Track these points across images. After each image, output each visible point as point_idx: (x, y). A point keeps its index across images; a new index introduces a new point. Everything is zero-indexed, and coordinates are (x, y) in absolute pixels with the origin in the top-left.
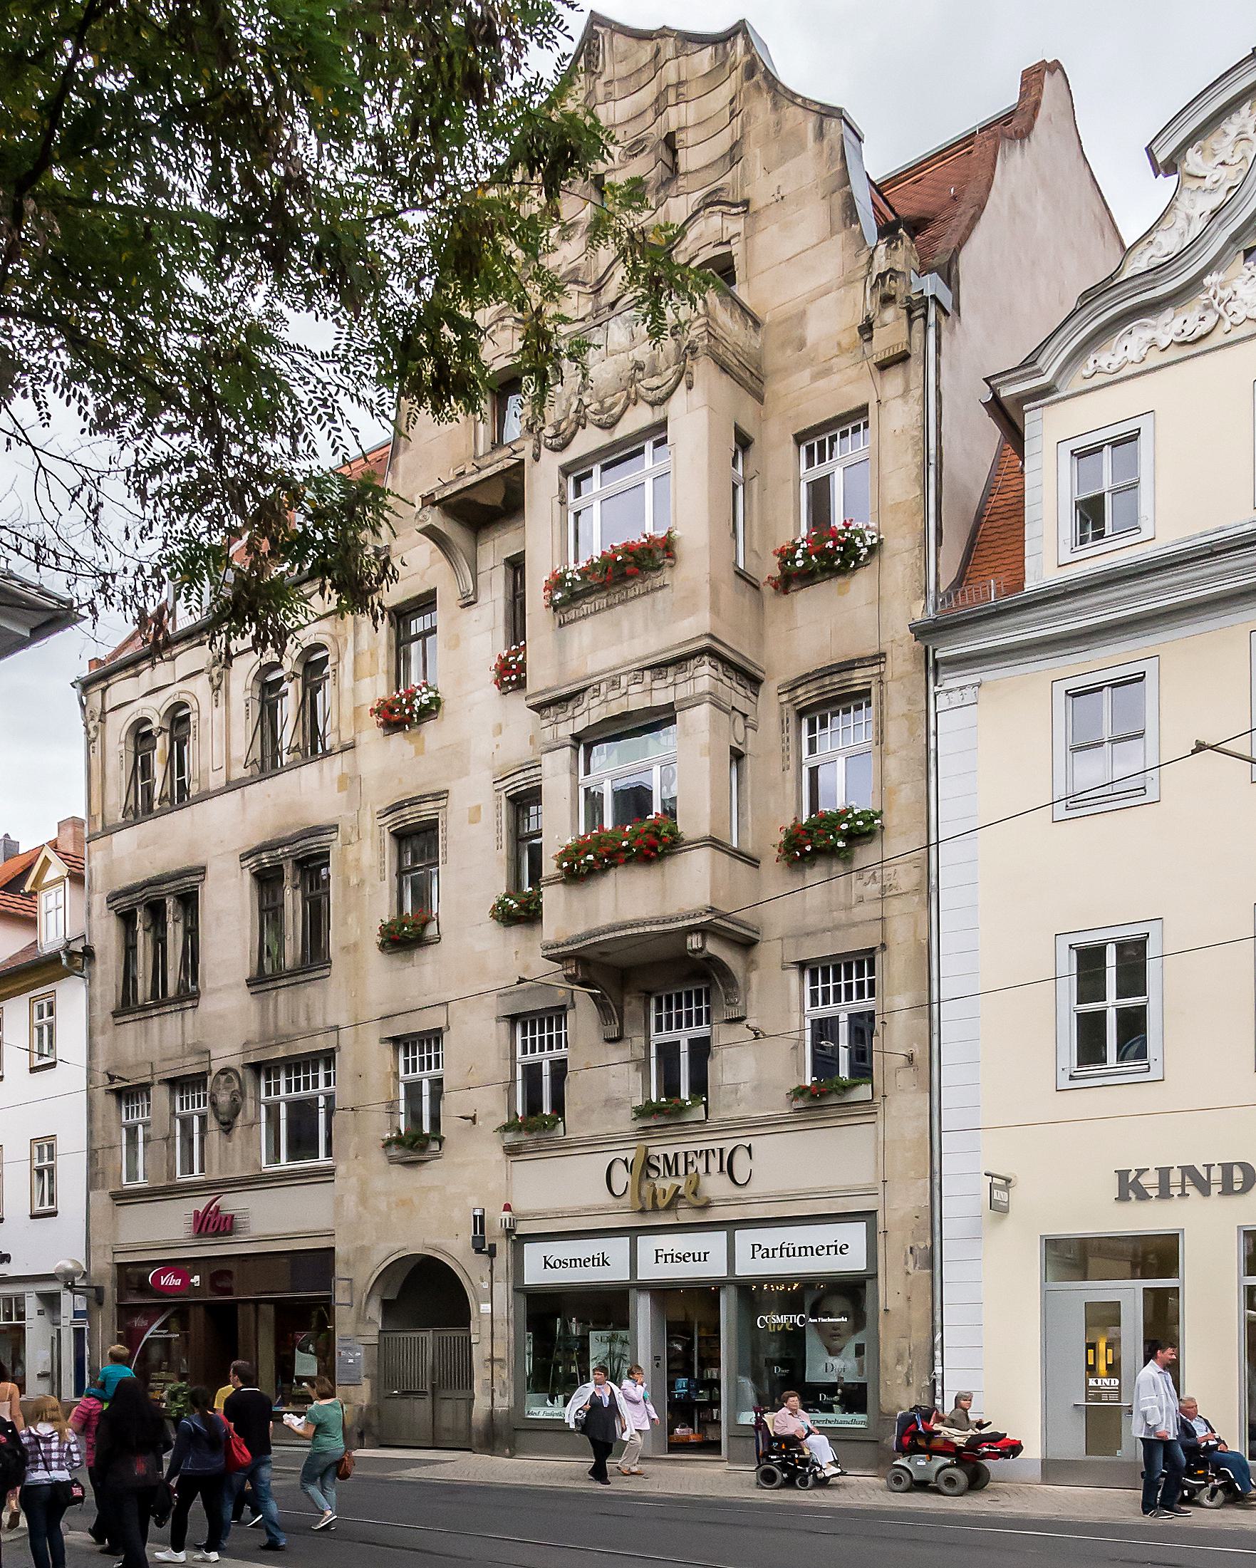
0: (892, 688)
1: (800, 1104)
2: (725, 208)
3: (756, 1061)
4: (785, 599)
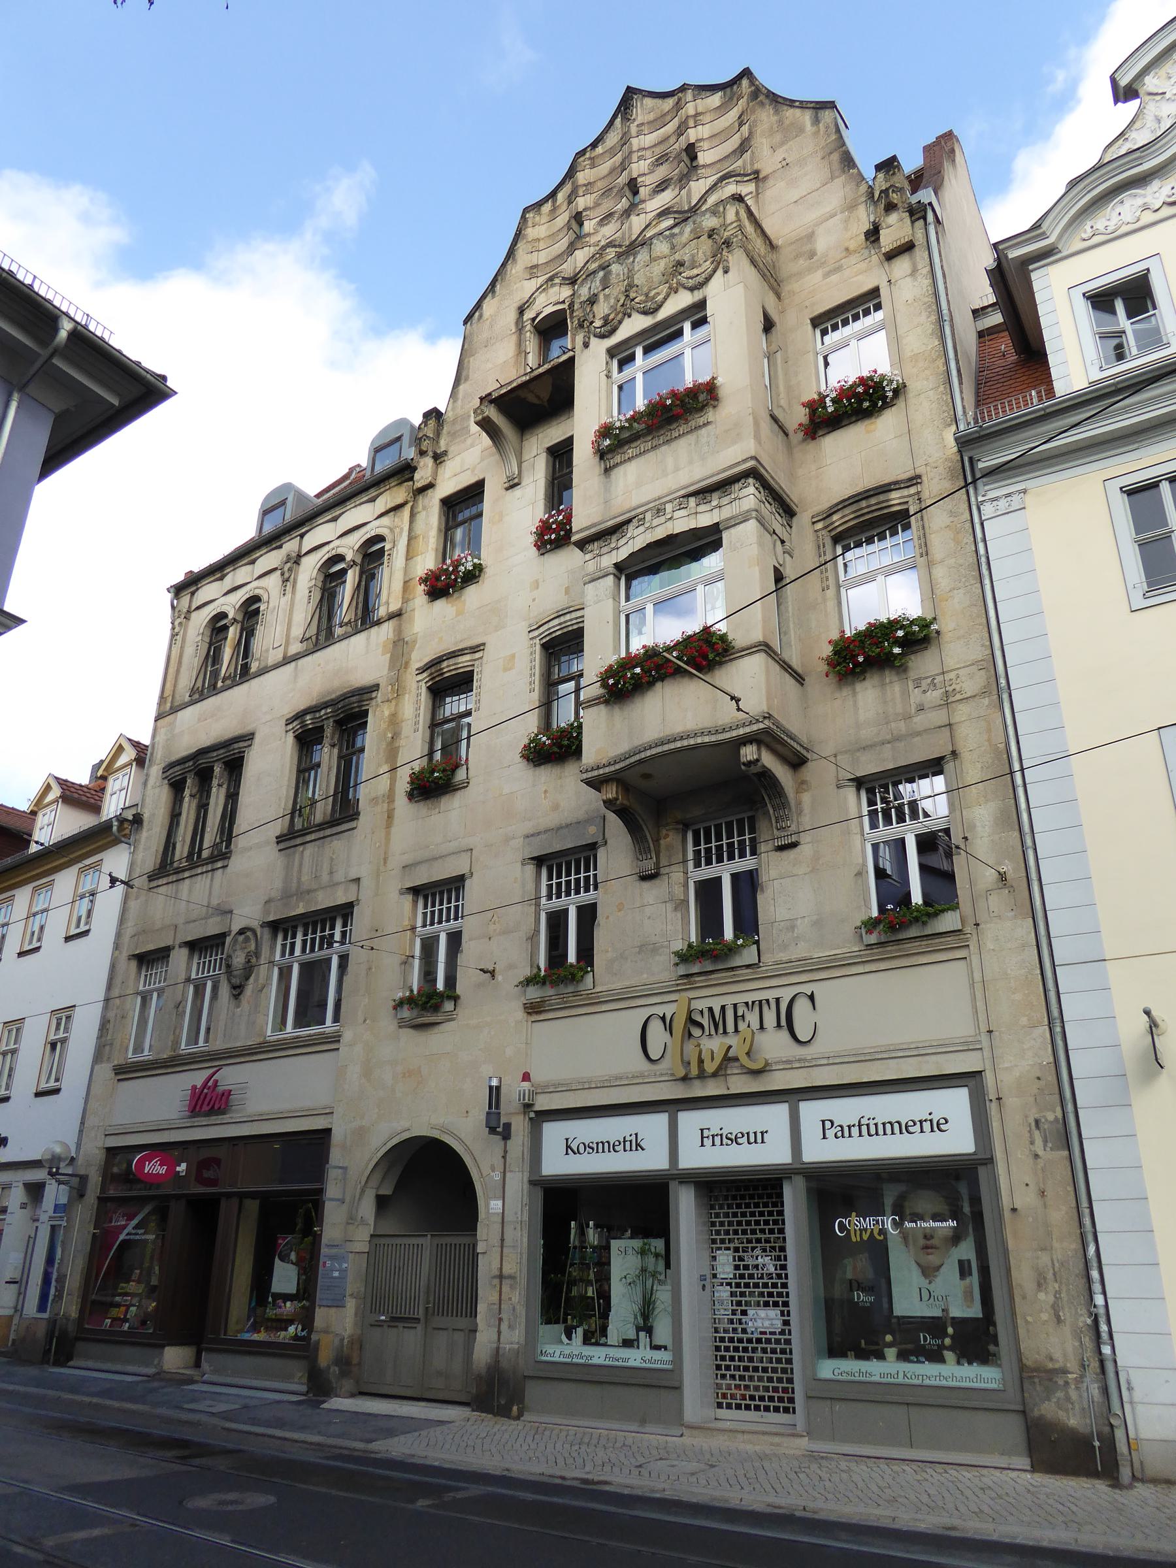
1: (873, 939)
2: (738, 179)
3: (817, 881)
4: (812, 445)
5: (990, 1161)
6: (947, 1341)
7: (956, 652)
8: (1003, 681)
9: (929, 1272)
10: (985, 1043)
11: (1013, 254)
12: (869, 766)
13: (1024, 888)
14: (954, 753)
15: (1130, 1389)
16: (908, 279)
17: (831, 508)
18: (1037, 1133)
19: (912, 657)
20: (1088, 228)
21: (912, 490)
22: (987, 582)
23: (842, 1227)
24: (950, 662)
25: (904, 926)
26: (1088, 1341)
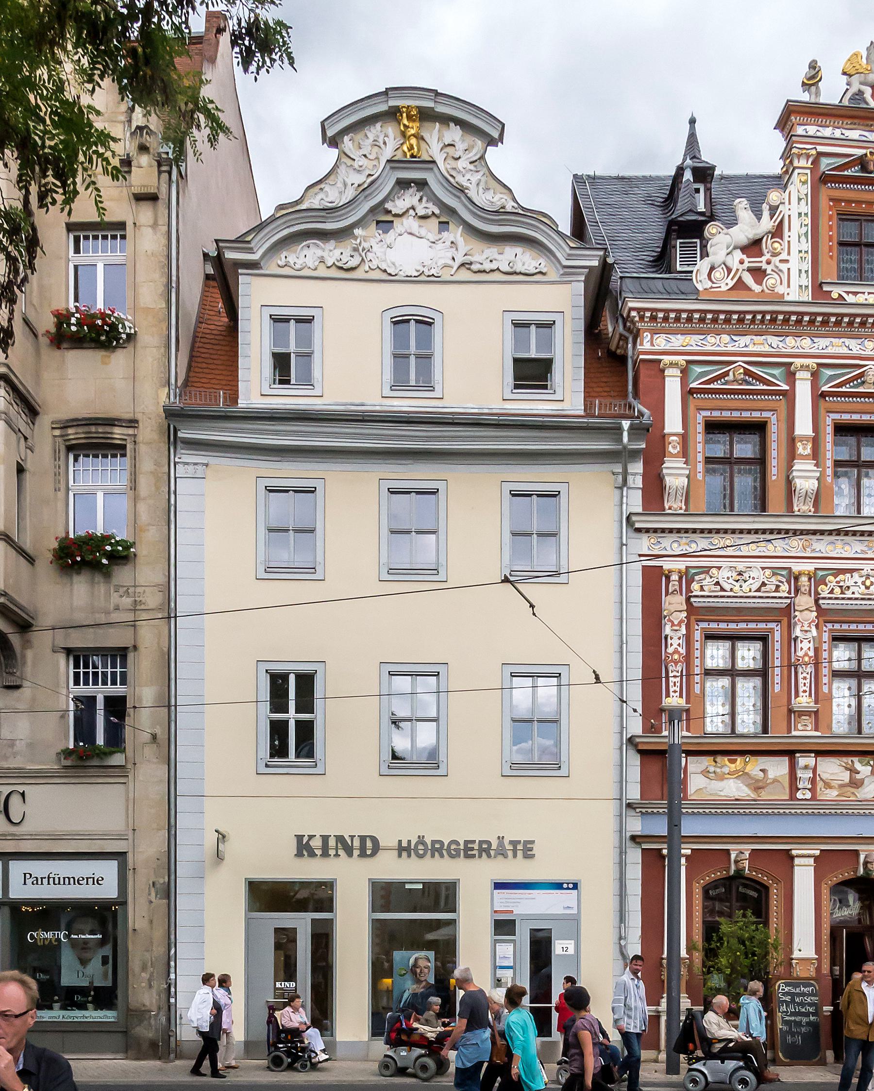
0: (143, 449)
5: (124, 903)
6: (90, 999)
7: (145, 574)
8: (173, 605)
9: (84, 962)
10: (130, 837)
11: (230, 255)
12: (78, 640)
13: (166, 745)
14: (135, 648)
15: (181, 1018)
16: (150, 230)
17: (68, 421)
18: (153, 890)
19: (116, 568)
20: (283, 256)
21: (130, 431)
22: (173, 526)
23: (32, 937)
24: (141, 580)
25: (89, 757)
26: (164, 996)
